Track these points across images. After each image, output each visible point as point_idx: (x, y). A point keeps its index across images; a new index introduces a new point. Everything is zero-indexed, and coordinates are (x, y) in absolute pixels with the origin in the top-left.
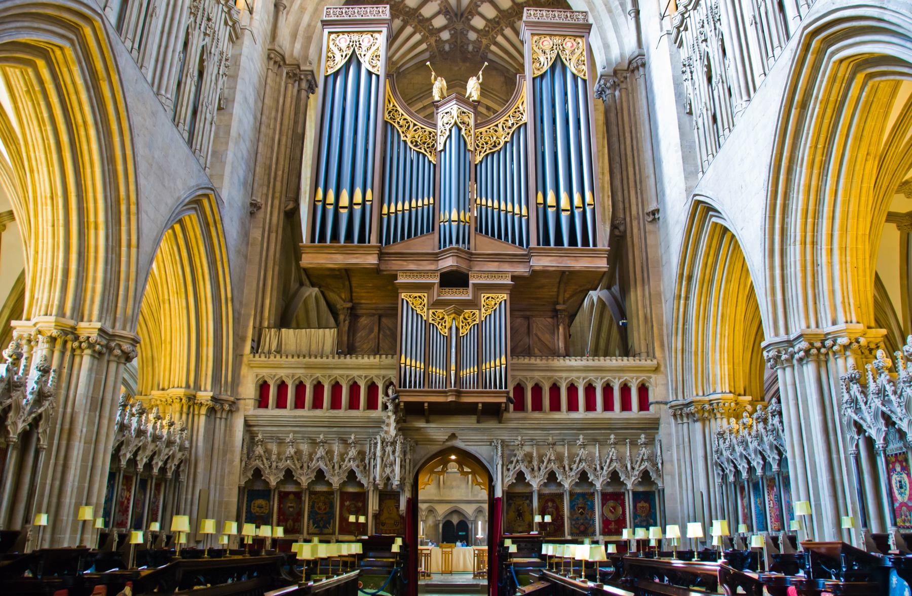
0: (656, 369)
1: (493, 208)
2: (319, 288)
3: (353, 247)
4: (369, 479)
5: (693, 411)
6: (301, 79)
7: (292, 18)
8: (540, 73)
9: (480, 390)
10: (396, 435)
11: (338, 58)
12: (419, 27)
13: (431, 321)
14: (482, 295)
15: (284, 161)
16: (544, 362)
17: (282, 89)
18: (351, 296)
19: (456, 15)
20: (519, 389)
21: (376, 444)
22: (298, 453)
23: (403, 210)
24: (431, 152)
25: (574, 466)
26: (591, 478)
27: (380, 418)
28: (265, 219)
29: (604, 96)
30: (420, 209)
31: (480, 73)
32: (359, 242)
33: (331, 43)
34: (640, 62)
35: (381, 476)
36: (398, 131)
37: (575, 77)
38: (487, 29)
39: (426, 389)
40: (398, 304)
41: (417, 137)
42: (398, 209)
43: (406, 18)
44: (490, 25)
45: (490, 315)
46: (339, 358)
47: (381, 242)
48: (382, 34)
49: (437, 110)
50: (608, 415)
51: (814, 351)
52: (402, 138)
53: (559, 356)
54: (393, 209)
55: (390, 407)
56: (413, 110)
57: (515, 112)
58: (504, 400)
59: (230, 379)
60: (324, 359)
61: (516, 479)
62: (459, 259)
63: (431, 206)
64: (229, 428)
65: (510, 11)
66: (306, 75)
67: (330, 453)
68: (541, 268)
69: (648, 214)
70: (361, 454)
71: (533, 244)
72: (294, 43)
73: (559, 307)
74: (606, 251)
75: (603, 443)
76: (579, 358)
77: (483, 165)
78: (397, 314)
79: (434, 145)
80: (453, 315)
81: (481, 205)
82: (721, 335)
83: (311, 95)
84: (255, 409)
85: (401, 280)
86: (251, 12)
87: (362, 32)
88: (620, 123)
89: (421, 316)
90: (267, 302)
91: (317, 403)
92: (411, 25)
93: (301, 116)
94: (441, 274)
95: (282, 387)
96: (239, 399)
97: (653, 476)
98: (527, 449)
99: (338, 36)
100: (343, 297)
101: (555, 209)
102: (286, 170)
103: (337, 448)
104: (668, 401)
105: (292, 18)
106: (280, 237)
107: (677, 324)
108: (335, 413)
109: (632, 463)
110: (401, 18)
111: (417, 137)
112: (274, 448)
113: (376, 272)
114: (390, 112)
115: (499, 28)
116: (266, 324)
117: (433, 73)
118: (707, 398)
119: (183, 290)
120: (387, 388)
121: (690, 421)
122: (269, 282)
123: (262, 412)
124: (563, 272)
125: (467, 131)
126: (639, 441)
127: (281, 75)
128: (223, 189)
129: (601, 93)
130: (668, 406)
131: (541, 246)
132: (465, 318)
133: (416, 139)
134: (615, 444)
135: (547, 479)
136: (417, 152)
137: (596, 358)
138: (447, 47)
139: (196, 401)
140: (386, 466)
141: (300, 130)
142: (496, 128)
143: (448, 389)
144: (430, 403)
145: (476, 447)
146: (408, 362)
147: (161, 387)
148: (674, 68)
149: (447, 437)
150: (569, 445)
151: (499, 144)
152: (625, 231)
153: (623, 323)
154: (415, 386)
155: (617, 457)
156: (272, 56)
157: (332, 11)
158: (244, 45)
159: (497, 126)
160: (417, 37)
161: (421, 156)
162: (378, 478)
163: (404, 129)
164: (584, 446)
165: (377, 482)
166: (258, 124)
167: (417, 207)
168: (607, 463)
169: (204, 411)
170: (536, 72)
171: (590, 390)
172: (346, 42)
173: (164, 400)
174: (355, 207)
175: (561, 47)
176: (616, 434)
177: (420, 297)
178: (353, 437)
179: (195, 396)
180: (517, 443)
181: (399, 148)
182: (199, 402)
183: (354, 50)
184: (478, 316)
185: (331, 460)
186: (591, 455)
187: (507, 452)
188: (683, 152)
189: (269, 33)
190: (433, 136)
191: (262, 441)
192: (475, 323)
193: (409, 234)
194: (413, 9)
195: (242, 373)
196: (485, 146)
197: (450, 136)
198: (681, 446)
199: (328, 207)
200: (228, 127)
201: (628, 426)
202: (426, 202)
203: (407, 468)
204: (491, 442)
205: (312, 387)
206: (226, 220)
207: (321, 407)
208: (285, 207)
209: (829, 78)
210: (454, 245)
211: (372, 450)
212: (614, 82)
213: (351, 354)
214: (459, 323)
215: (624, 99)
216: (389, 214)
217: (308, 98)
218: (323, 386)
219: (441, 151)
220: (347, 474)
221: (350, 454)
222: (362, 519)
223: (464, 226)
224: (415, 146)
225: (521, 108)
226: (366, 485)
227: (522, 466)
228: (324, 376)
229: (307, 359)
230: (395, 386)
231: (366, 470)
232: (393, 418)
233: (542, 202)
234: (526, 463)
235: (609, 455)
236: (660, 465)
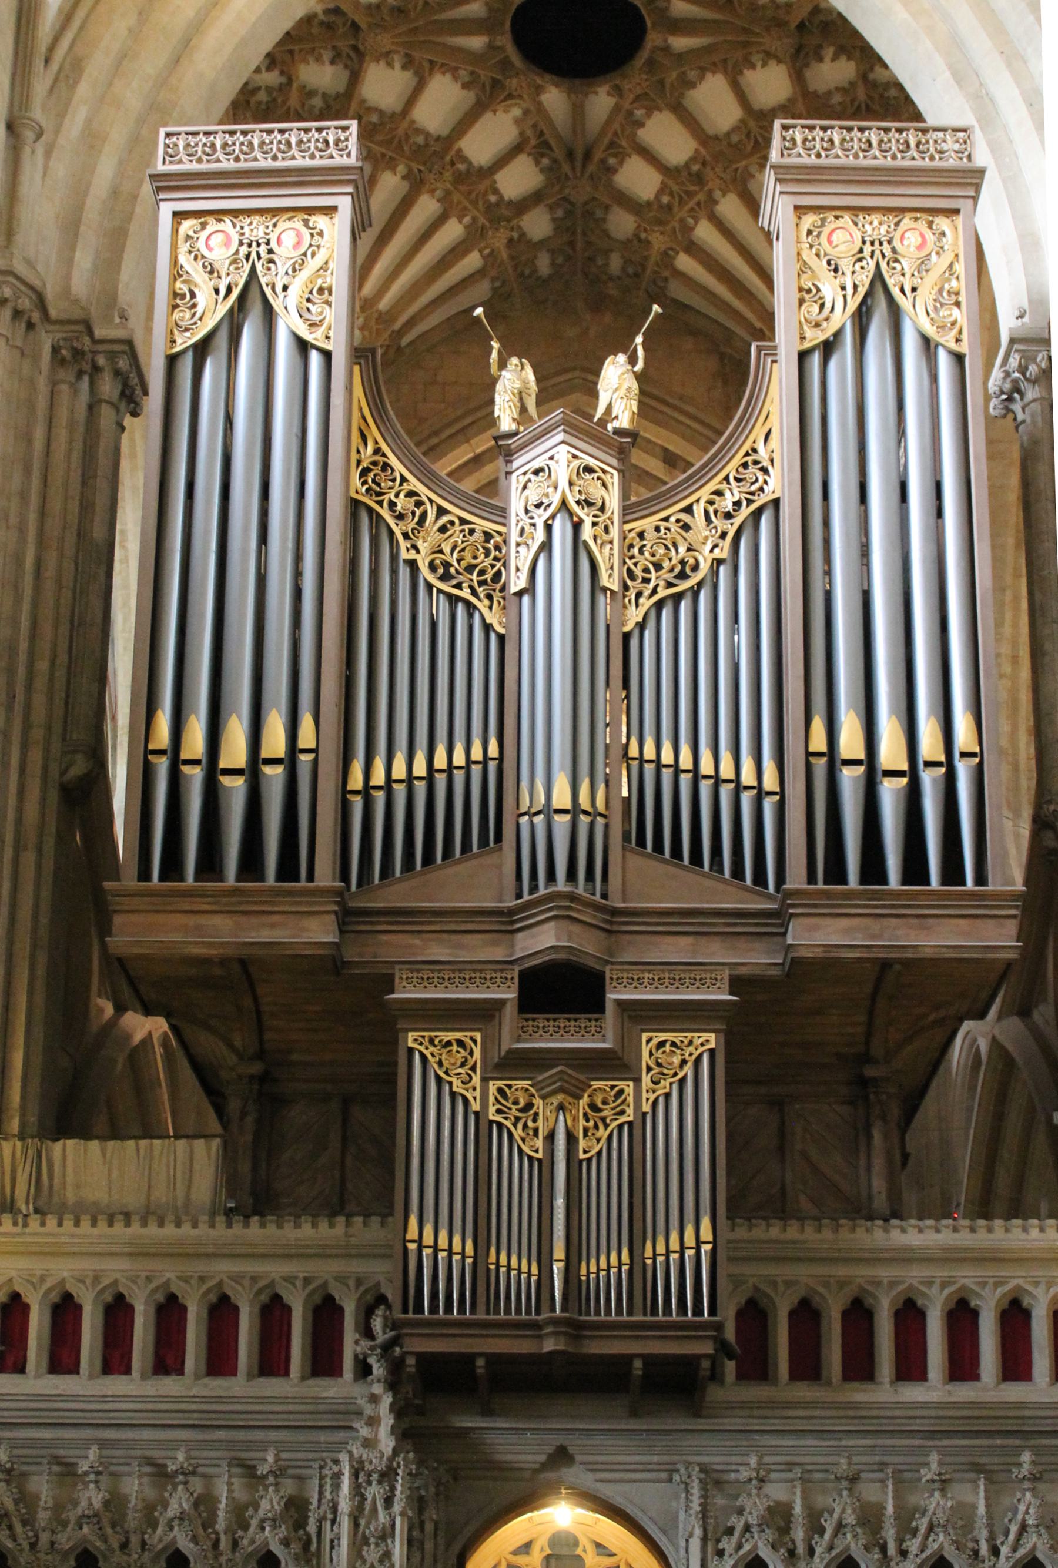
1: (677, 771)
2: (168, 1017)
3: (261, 892)
8: (821, 337)
9: (638, 1318)
10: (396, 1452)
14: (645, 1036)
15: (56, 628)
16: (827, 1234)
18: (261, 1042)
21: (338, 1476)
22: (115, 1503)
23: (410, 779)
24: (489, 597)
27: (350, 1401)
29: (1017, 407)
31: (639, 339)
32: (281, 877)
36: (391, 533)
39: (481, 1316)
40: (395, 1064)
41: (447, 549)
42: (395, 776)
45: (668, 1096)
47: (345, 876)
49: (509, 462)
52: (404, 555)
54: (379, 777)
56: (443, 467)
57: (745, 465)
58: (707, 1348)
60: (186, 1229)
62: (576, 928)
63: (492, 766)
67: (205, 1503)
68: (819, 953)
72: (73, 248)
74: (1014, 896)
76: (930, 1222)
78: (393, 1096)
79: (498, 574)
81: (641, 759)
83: (128, 420)
87: (275, 212)
89: (466, 1101)
93: (102, 484)
94: (523, 974)
98: (777, 1492)
99: (204, 225)
100: (238, 1043)
101: (862, 769)
106: (49, 865)
108: (218, 1386)
111: (447, 549)
114: (365, 472)
117: (495, 345)
124: (885, 965)
125: (599, 529)
127: (36, 358)
129: (1010, 399)
131: (821, 886)
132: (593, 1107)
134: (1035, 1478)
136: (453, 600)
137: (982, 1222)
140: (366, 1541)
142: (683, 516)
143: (545, 1315)
144: (493, 1359)
145: (627, 1487)
146: (428, 1239)
150: (898, 1482)
151: (695, 568)
154: (449, 1308)
155: (1040, 1518)
157: (181, 144)
159: (688, 510)
161: (460, 608)
163: (410, 525)
168: (1012, 1537)
174: (268, 770)
176: (1036, 1451)
177: (460, 1043)
178: (271, 1459)
180: (744, 1474)
181: (394, 572)
184: (631, 1099)
185: (208, 1523)
190: (498, 548)
192: (623, 1119)
202: (477, 754)
203: (429, 1546)
205: (152, 1310)
210: (561, 884)
211: (328, 1495)
213: (262, 1215)
214: (575, 1119)
216: (367, 791)
217: (123, 429)
218: (184, 1309)
219: (520, 594)
221: (265, 1505)
223: (592, 825)
224: (442, 578)
225: (763, 454)
228: (186, 1280)
229: (136, 1228)
230: (389, 1307)
232: (387, 1400)
233: (823, 748)
234: (770, 1534)
235: (1015, 1511)
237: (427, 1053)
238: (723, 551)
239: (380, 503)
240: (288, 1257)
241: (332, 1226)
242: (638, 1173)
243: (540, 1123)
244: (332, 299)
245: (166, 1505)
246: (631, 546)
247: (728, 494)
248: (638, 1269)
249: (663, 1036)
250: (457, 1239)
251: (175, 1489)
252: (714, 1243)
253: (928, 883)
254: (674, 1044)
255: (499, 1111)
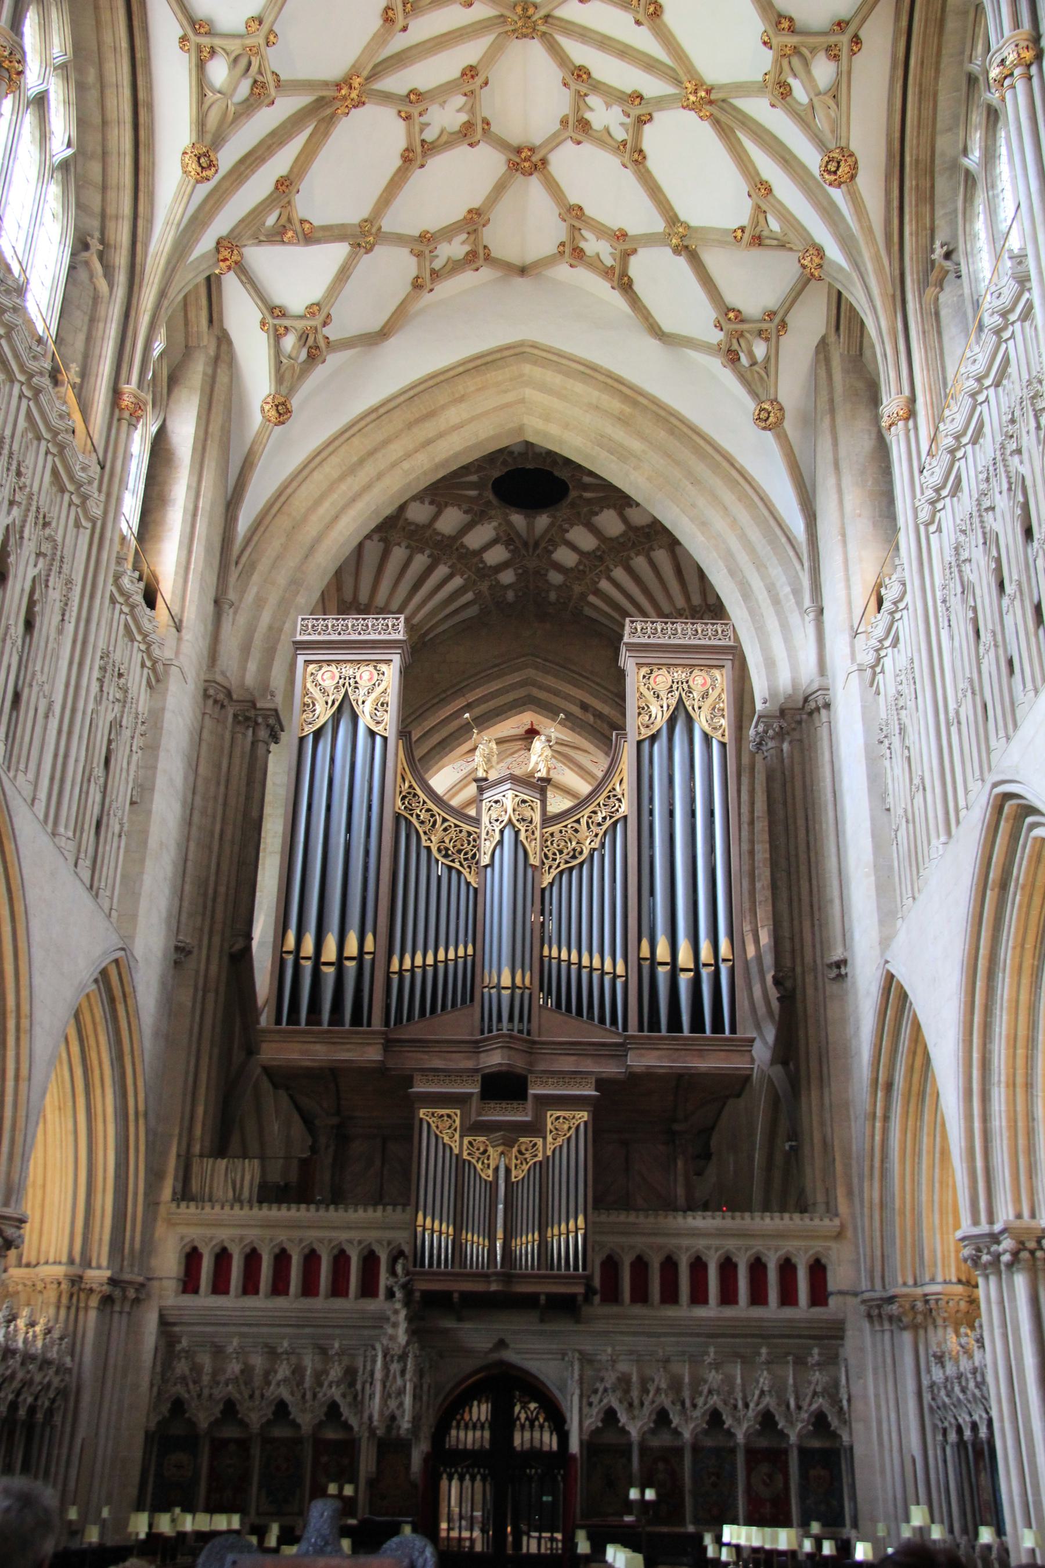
0: (839, 1236)
4: (361, 1418)
5: (896, 1313)
6: (256, 723)
7: (242, 619)
9: (543, 1272)
10: (408, 1343)
11: (319, 708)
12: (459, 566)
13: (465, 1156)
14: (549, 1113)
17: (227, 744)
19: (526, 544)
20: (611, 1265)
22: (247, 1371)
24: (469, 867)
25: (700, 1401)
26: (728, 1422)
28: (197, 972)
30: (451, 964)
33: (309, 679)
34: (820, 703)
35: (381, 1413)
37: (707, 739)
38: (581, 567)
39: (457, 1270)
41: (447, 841)
43: (435, 552)
44: (587, 563)
46: (317, 1210)
48: (392, 664)
50: (758, 1312)
51: (1025, 1255)
52: (424, 843)
53: (676, 1210)
54: (407, 965)
55: (399, 1295)
57: (609, 797)
59: (137, 1245)
61: (602, 1421)
63: (469, 959)
64: (134, 1330)
65: (621, 540)
66: (266, 717)
67: (298, 1371)
68: (643, 1069)
69: (829, 966)
70: (350, 1374)
71: (632, 1030)
73: (676, 1127)
75: (747, 1361)
77: (555, 889)
79: (474, 855)
80: (500, 1149)
82: (941, 1183)
84: (176, 1296)
85: (420, 1087)
86: (178, 630)
88: (789, 800)
89: (451, 1148)
90: (200, 1110)
91: (279, 1287)
92: (445, 564)
95: (222, 1257)
96: (149, 1279)
97: (834, 1422)
101: (668, 967)
102: (233, 884)
103: (310, 1362)
104: (859, 1290)
105: (242, 619)
107: (872, 1160)
109: (797, 1398)
110: (427, 552)
111: (447, 841)
112: (205, 1360)
113: (380, 1071)
115: (602, 568)
116: (197, 1149)
118: (919, 1291)
119: (70, 1104)
120: (393, 1261)
121: (894, 1327)
122: (203, 1076)
123: (188, 1300)
124: (680, 1076)
125: (529, 833)
126: (810, 1359)
128: (137, 940)
130: (859, 1299)
133: (447, 845)
135: (655, 1422)
136: (450, 868)
138: (510, 596)
139: (83, 1286)
140: (389, 1396)
141: (255, 814)
142: (575, 825)
143: (492, 1270)
147: (24, 1261)
148: (867, 730)
149: (490, 1345)
151: (581, 853)
152: (794, 989)
153: (791, 1147)
156: (211, 692)
158: (170, 693)
160: (457, 581)
162: (376, 1417)
164: (717, 1366)
165: (375, 1423)
166: (188, 812)
167: (447, 960)
169: (94, 1302)
170: (643, 730)
171: (728, 1267)
172: (333, 678)
173: (29, 1283)
175: (685, 686)
177: (449, 1116)
178: (337, 1345)
179: (81, 1277)
182: (88, 1286)
183: (346, 691)
184: (541, 1149)
185: (300, 1383)
186: (729, 1380)
187: (589, 1373)
188: (878, 878)
189: (205, 653)
190: (475, 840)
191: (187, 1352)
193: (431, 1008)
194: (449, 537)
195: (157, 1235)
196: (558, 856)
197: (501, 843)
198: (881, 1370)
199: (303, 962)
200: (145, 833)
201: (792, 1332)
202: (461, 953)
203: (425, 1398)
204: (564, 1355)
205: (272, 1257)
206: (141, 989)
207: (286, 1292)
208: (231, 947)
209: (1030, 857)
211: (369, 1368)
212: (781, 728)
214: (510, 1159)
215: (797, 759)
216: (401, 972)
219: (486, 867)
220: (324, 1409)
222: (348, 1490)
223: (522, 995)
226: (356, 1429)
227: (613, 1399)
231: (357, 1403)
232: (403, 1313)
233: (648, 956)
236: (845, 1403)
237: (430, 1121)
238: (596, 845)
239: (411, 815)
240: (350, 1228)
241: (375, 1211)
242: (544, 1190)
243: (491, 1161)
244: (389, 709)
245: (276, 1372)
246: (546, 841)
247: (599, 814)
248: (543, 1244)
249: (559, 1113)
250: (444, 1226)
251: (281, 1363)
252: (586, 1229)
253: (704, 1032)
254: (564, 1118)
255: (469, 1154)
